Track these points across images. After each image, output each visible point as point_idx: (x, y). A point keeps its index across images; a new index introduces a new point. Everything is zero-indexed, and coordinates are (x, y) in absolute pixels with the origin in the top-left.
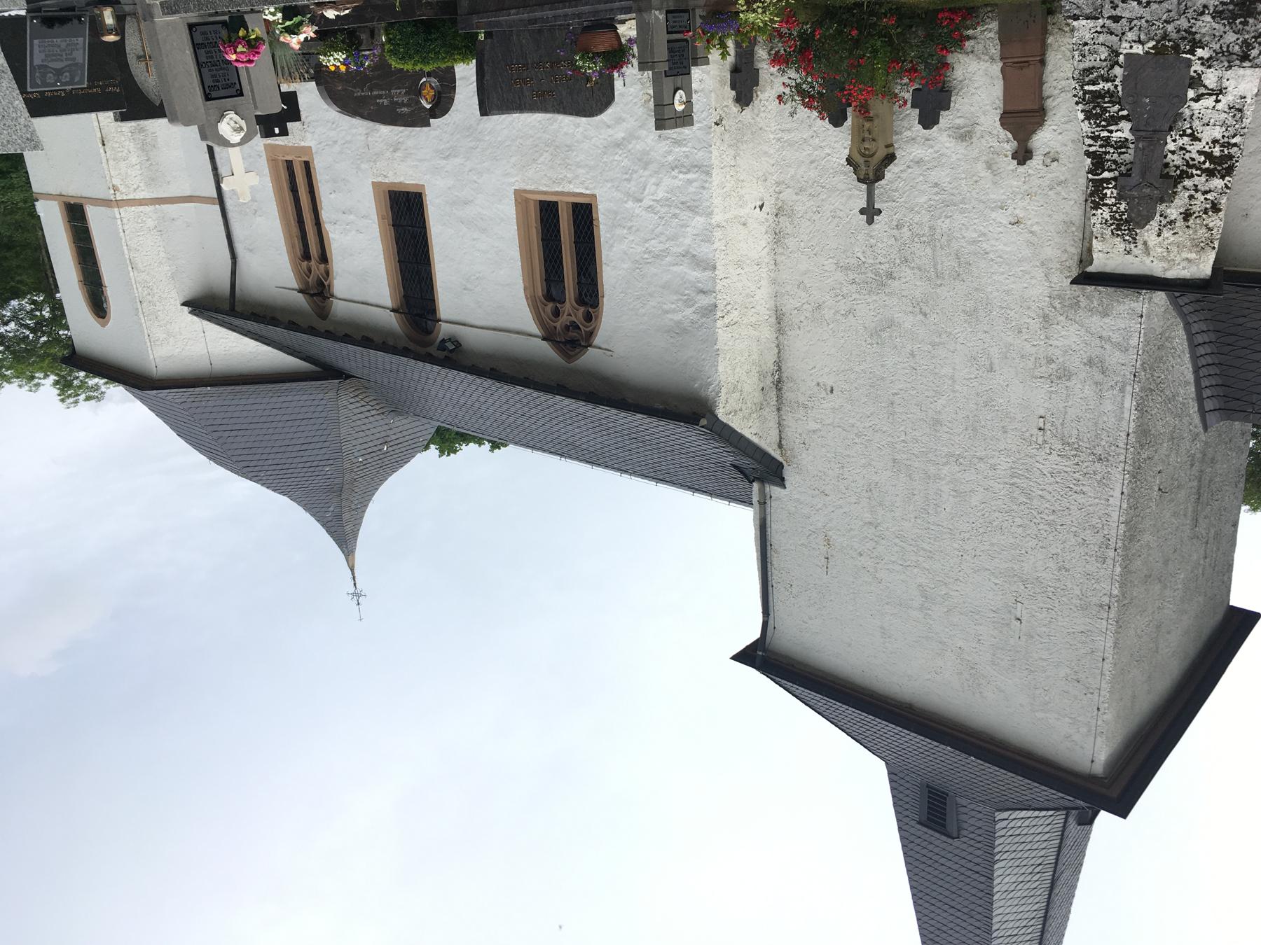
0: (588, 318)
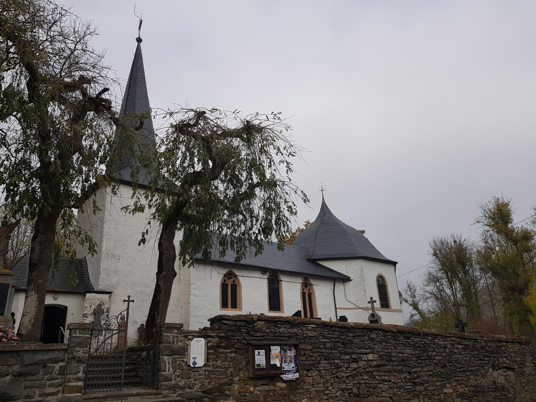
0: (225, 281)
